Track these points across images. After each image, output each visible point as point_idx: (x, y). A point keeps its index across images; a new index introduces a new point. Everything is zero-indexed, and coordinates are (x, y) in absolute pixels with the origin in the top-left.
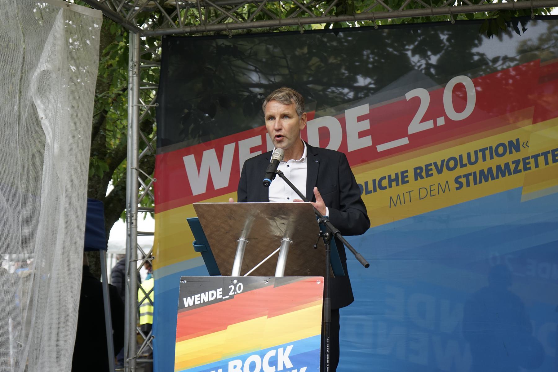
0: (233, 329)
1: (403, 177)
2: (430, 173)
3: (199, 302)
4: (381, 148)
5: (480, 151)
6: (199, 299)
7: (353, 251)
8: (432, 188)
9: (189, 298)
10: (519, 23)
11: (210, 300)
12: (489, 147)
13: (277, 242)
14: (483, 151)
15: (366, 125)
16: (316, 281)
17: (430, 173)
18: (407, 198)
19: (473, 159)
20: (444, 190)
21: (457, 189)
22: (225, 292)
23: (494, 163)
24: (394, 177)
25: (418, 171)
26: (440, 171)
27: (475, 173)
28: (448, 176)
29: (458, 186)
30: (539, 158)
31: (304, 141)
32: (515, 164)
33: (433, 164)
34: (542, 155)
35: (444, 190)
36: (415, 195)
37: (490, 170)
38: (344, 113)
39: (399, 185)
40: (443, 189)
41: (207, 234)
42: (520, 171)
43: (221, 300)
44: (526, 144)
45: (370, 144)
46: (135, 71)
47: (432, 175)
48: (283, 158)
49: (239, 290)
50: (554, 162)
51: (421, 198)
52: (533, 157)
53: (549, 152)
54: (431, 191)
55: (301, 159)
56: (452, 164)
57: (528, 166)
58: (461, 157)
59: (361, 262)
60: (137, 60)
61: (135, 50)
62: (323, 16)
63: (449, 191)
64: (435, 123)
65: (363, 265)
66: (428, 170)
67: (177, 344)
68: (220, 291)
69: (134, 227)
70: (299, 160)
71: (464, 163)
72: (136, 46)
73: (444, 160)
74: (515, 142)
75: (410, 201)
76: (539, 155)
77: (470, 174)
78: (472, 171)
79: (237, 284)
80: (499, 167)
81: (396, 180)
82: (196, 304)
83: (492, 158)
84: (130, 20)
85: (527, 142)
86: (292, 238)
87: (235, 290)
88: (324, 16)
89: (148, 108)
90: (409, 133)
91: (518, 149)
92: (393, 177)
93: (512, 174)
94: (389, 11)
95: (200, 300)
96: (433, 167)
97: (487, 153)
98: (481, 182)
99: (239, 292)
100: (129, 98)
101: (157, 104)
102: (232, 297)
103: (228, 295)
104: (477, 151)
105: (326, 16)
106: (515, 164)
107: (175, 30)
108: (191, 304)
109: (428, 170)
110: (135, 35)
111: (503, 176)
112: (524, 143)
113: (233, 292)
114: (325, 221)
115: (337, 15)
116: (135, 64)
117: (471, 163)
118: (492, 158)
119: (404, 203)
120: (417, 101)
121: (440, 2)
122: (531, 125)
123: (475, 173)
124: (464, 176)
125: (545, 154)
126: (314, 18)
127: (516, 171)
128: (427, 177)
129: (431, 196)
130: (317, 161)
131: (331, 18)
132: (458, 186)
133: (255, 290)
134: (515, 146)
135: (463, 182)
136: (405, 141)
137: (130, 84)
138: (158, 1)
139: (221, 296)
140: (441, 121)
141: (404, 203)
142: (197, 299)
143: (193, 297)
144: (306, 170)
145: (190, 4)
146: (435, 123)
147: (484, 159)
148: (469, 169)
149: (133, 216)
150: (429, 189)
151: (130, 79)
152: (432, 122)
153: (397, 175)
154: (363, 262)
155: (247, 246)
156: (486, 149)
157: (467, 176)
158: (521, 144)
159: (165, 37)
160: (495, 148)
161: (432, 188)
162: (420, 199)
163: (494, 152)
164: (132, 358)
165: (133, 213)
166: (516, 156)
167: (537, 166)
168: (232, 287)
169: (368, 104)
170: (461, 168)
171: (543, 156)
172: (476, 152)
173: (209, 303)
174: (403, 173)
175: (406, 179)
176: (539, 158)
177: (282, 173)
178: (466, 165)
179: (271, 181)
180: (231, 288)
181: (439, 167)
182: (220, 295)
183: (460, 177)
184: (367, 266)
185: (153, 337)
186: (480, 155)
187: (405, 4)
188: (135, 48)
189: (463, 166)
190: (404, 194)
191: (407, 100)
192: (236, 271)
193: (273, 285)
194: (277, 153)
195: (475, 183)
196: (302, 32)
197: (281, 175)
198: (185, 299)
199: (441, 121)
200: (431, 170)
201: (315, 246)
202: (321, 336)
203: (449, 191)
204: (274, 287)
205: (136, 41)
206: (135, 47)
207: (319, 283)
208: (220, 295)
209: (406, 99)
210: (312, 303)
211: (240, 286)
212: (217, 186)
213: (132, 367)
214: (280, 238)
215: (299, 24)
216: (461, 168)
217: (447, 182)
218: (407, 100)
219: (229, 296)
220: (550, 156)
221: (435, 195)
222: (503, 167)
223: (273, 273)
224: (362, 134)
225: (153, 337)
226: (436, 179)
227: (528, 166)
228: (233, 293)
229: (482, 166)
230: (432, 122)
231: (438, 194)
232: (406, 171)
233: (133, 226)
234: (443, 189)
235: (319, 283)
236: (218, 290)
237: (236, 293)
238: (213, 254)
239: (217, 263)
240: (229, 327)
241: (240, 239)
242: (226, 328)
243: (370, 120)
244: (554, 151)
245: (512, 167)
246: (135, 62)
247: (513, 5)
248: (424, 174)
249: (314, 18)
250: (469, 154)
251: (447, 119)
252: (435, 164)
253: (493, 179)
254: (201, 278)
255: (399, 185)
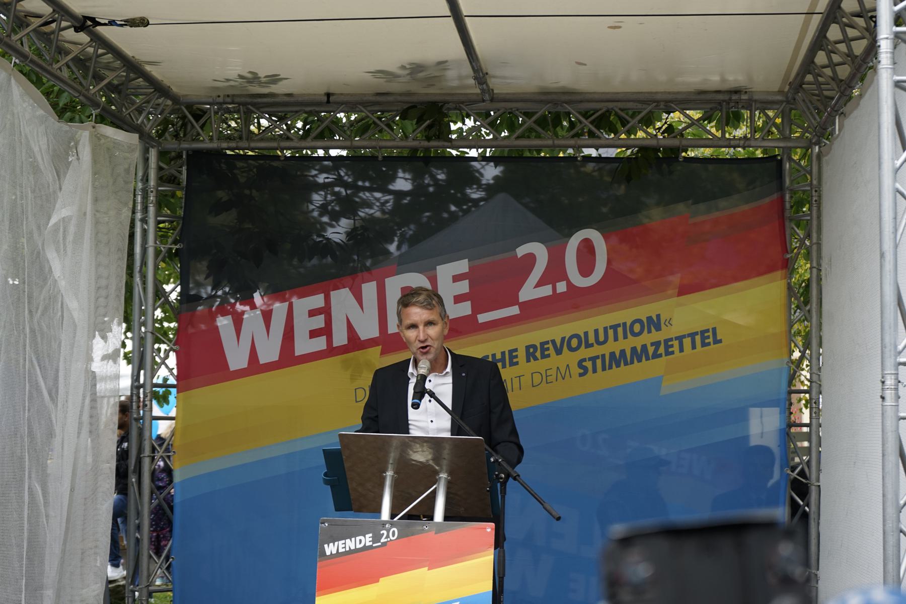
0: (386, 583)
1: (512, 357)
2: (546, 353)
3: (344, 550)
4: (483, 318)
5: (611, 327)
6: (344, 546)
7: (540, 499)
8: (549, 373)
9: (331, 544)
10: (664, 166)
11: (357, 547)
12: (623, 323)
13: (432, 479)
14: (615, 327)
15: (464, 287)
16: (486, 528)
17: (546, 353)
18: (516, 385)
19: (601, 338)
20: (563, 376)
21: (581, 375)
22: (376, 538)
23: (627, 344)
24: (500, 357)
25: (531, 350)
26: (559, 352)
27: (603, 356)
28: (570, 358)
29: (582, 371)
30: (684, 340)
31: (448, 348)
32: (654, 347)
33: (550, 342)
34: (688, 337)
35: (563, 376)
36: (527, 380)
37: (623, 352)
38: (436, 269)
39: (505, 367)
40: (563, 374)
41: (347, 465)
42: (660, 356)
43: (371, 547)
44: (669, 322)
45: (469, 312)
46: (151, 199)
47: (548, 356)
48: (430, 372)
49: (393, 535)
50: (702, 346)
51: (534, 385)
52: (676, 338)
53: (696, 333)
54: (547, 376)
55: (445, 372)
56: (574, 343)
57: (671, 350)
58: (586, 334)
59: (551, 514)
60: (155, 185)
61: (152, 170)
62: (410, 140)
63: (571, 377)
64: (554, 289)
65: (554, 518)
66: (543, 350)
67: (316, 598)
68: (370, 537)
69: (147, 411)
70: (443, 374)
71: (590, 342)
72: (152, 164)
73: (565, 337)
74: (655, 318)
75: (520, 389)
76: (684, 336)
77: (598, 357)
78: (600, 354)
79: (391, 529)
80: (634, 349)
81: (503, 360)
82: (340, 551)
83: (625, 337)
84: (150, 131)
85: (671, 319)
86: (450, 473)
87: (388, 536)
88: (412, 140)
89: (166, 249)
90: (521, 300)
91: (658, 328)
92: (498, 356)
93: (649, 359)
94: (498, 139)
95: (345, 547)
96: (550, 346)
97: (620, 330)
98: (610, 368)
99: (392, 538)
100: (137, 231)
101: (180, 245)
102: (384, 544)
103: (380, 542)
104: (607, 327)
105: (413, 139)
106: (654, 347)
107: (206, 143)
108: (334, 552)
109: (543, 350)
110: (153, 150)
111: (640, 361)
112: (666, 320)
113: (385, 538)
114: (500, 460)
115: (428, 139)
116: (152, 189)
117: (599, 343)
118: (625, 337)
119: (512, 391)
120: (531, 259)
121: (560, 126)
122: (676, 299)
123: (603, 356)
124: (590, 359)
125: (692, 335)
126: (398, 141)
127: (656, 355)
128: (542, 358)
129: (547, 383)
130: (464, 374)
131: (420, 143)
132: (582, 371)
133: (413, 537)
134: (654, 323)
135: (588, 366)
136: (514, 310)
137: (137, 212)
138: (185, 105)
139: (371, 543)
140: (562, 287)
141: (512, 391)
142: (341, 546)
143: (336, 543)
144: (451, 385)
145: (224, 109)
146: (554, 289)
147: (616, 339)
148: (596, 350)
149: (147, 396)
150: (545, 374)
151: (138, 206)
152: (550, 287)
153: (503, 353)
154: (553, 514)
155: (395, 480)
156: (619, 325)
157: (593, 359)
158: (662, 322)
159: (190, 153)
160: (629, 324)
161: (549, 373)
162: (533, 386)
163: (629, 330)
164: (144, 586)
165: (147, 392)
166: (655, 336)
167: (681, 350)
168: (385, 532)
169: (467, 260)
170: (586, 347)
171: (690, 338)
172: (605, 329)
173: (357, 551)
174: (511, 352)
175: (515, 360)
176: (684, 340)
177: (434, 393)
178: (592, 345)
179: (421, 401)
180: (383, 534)
181: (558, 345)
182: (370, 541)
183: (584, 360)
184: (559, 519)
185: (173, 558)
186: (611, 333)
187: (519, 132)
188: (151, 168)
189: (588, 345)
190: (512, 379)
191: (519, 256)
192: (385, 514)
193: (434, 532)
194: (423, 366)
195: (604, 369)
196: (380, 158)
197: (432, 395)
198: (326, 546)
199: (562, 287)
200: (548, 349)
201: (488, 489)
202: (491, 593)
203: (571, 377)
204: (436, 533)
205: (153, 157)
206: (152, 167)
207: (489, 530)
208: (370, 541)
209: (517, 256)
210: (482, 553)
211: (394, 532)
212: (263, 359)
213: (144, 599)
214: (437, 473)
215: (378, 148)
216: (586, 348)
217: (568, 365)
218: (519, 256)
219: (382, 543)
220: (698, 338)
221: (552, 382)
222: (639, 350)
223: (431, 518)
224: (458, 299)
225: (173, 558)
226: (554, 361)
227: (671, 350)
228: (386, 540)
229: (612, 347)
230: (550, 287)
231: (557, 380)
232: (516, 350)
233: (147, 410)
234: (563, 374)
235: (489, 530)
236: (367, 536)
237: (389, 539)
238: (349, 488)
239: (352, 497)
240: (382, 580)
241: (387, 473)
242: (378, 581)
243: (469, 281)
244: (703, 332)
245: (651, 350)
246: (152, 187)
247: (658, 142)
248: (538, 354)
249: (398, 141)
250: (596, 331)
251: (569, 284)
252: (553, 342)
253: (626, 364)
254: (346, 521)
255: (505, 367)
